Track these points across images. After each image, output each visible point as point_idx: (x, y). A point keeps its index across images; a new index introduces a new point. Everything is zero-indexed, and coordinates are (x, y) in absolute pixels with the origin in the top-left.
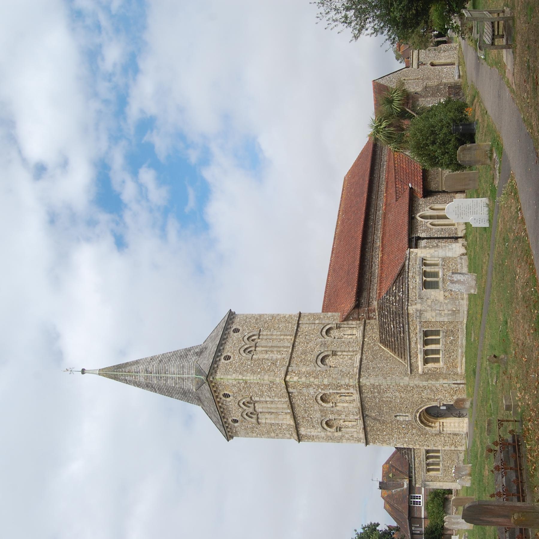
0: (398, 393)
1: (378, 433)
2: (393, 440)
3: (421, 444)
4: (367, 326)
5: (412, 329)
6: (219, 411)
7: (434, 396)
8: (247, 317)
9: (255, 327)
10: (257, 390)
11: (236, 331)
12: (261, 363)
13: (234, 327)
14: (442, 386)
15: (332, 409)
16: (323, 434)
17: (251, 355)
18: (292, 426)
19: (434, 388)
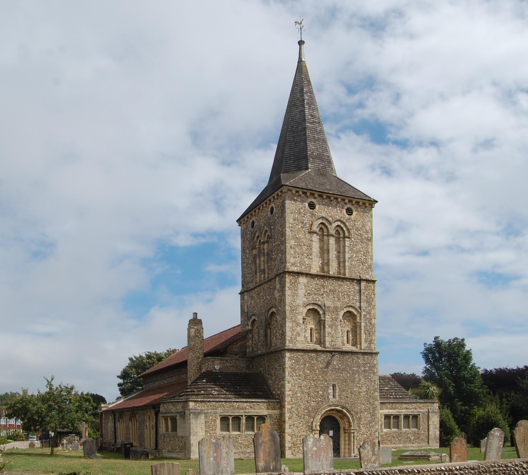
0: (366, 389)
1: (307, 365)
2: (297, 380)
3: (293, 410)
15: (339, 320)
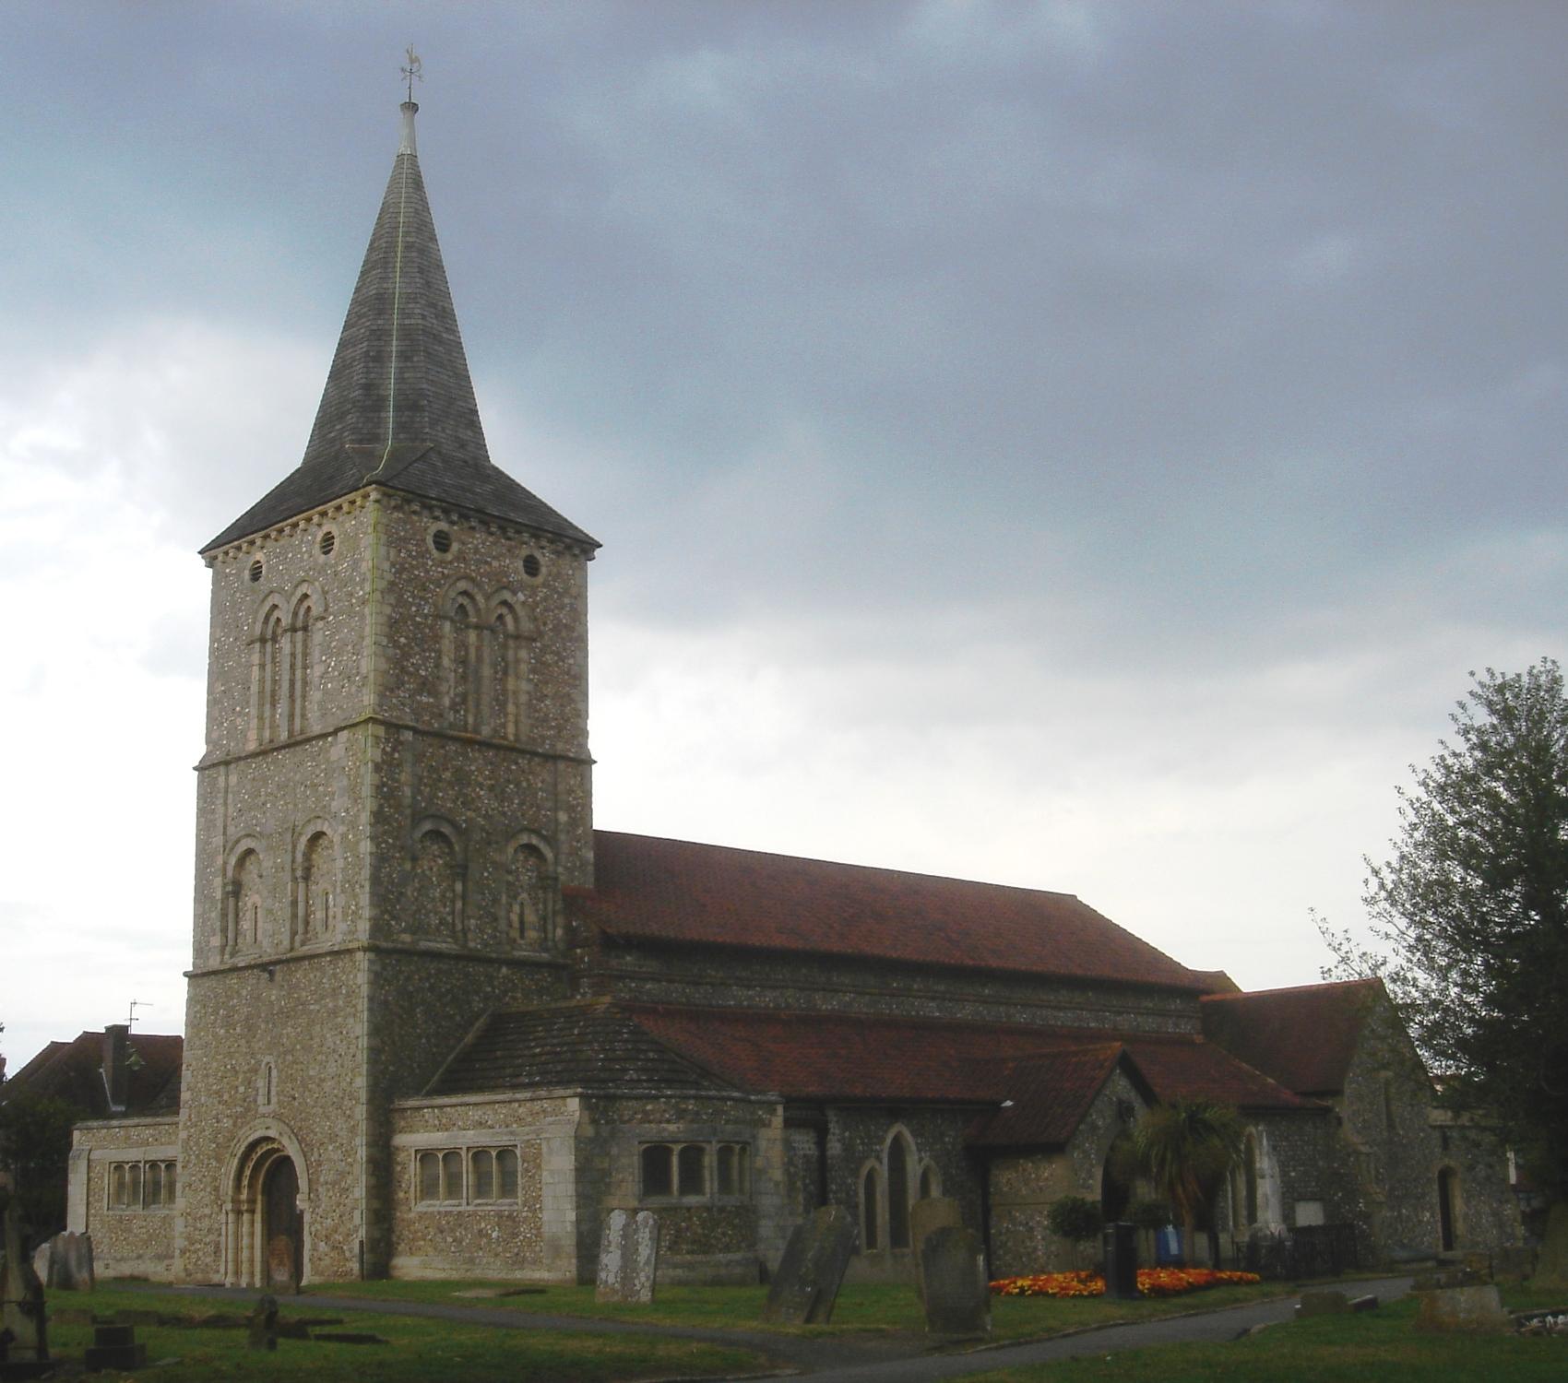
4: (550, 976)
5: (521, 1110)
6: (285, 523)
7: (327, 1183)
8: (576, 598)
9: (545, 624)
10: (342, 635)
11: (532, 566)
12: (426, 647)
13: (544, 558)
14: (353, 1209)
16: (218, 840)
17: (453, 614)
18: (241, 745)
19: (349, 1182)
